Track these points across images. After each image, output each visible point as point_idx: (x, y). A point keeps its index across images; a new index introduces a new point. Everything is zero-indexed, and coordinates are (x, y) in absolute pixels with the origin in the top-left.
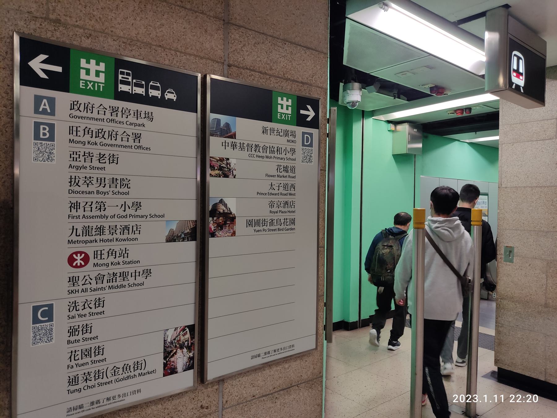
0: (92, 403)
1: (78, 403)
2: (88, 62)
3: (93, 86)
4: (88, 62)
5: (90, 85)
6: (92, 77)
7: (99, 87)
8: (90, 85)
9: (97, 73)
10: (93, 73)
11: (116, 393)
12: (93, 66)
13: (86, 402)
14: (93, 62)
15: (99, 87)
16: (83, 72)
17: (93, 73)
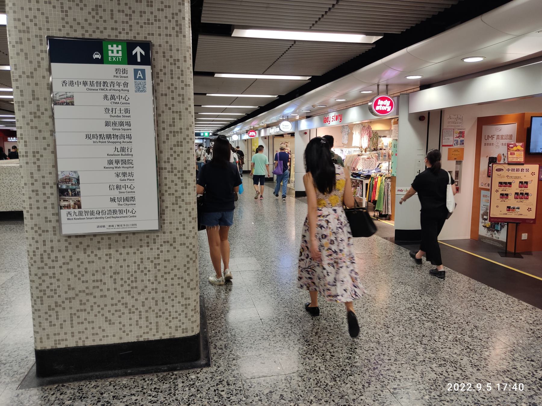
0: (110, 226)
1: (103, 224)
2: (112, 46)
3: (116, 59)
4: (112, 46)
5: (114, 59)
6: (115, 54)
7: (119, 59)
8: (114, 59)
9: (118, 53)
10: (115, 52)
11: (122, 223)
12: (115, 48)
13: (107, 225)
14: (115, 46)
15: (119, 59)
16: (110, 52)
17: (115, 52)
